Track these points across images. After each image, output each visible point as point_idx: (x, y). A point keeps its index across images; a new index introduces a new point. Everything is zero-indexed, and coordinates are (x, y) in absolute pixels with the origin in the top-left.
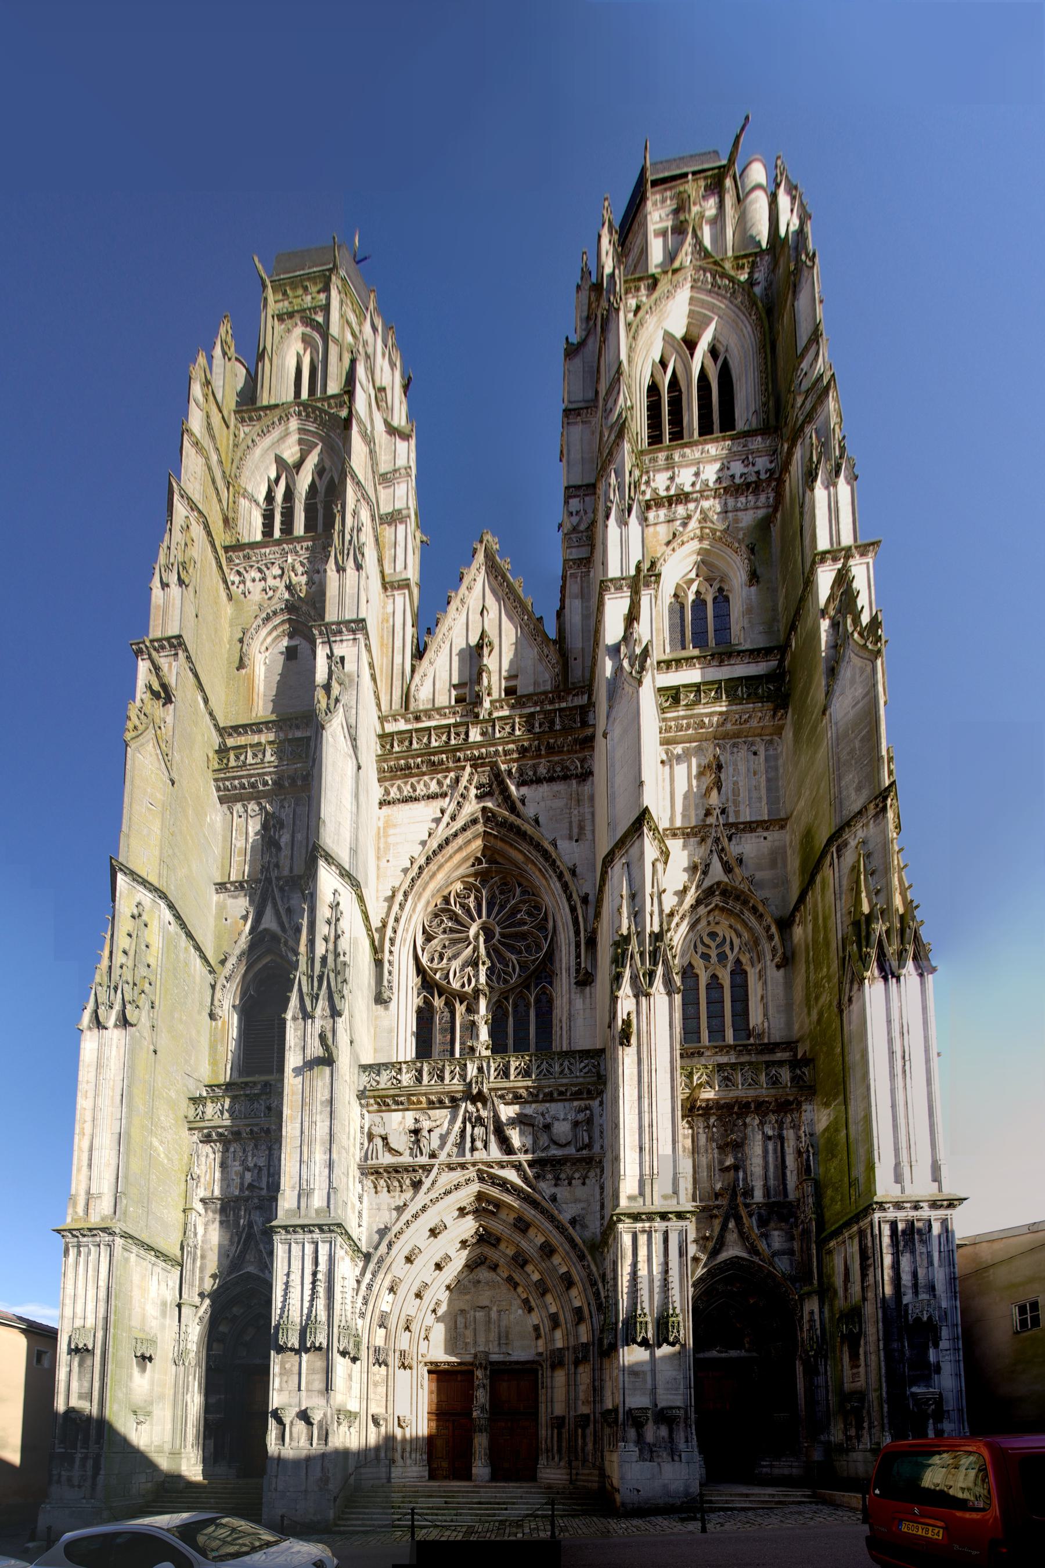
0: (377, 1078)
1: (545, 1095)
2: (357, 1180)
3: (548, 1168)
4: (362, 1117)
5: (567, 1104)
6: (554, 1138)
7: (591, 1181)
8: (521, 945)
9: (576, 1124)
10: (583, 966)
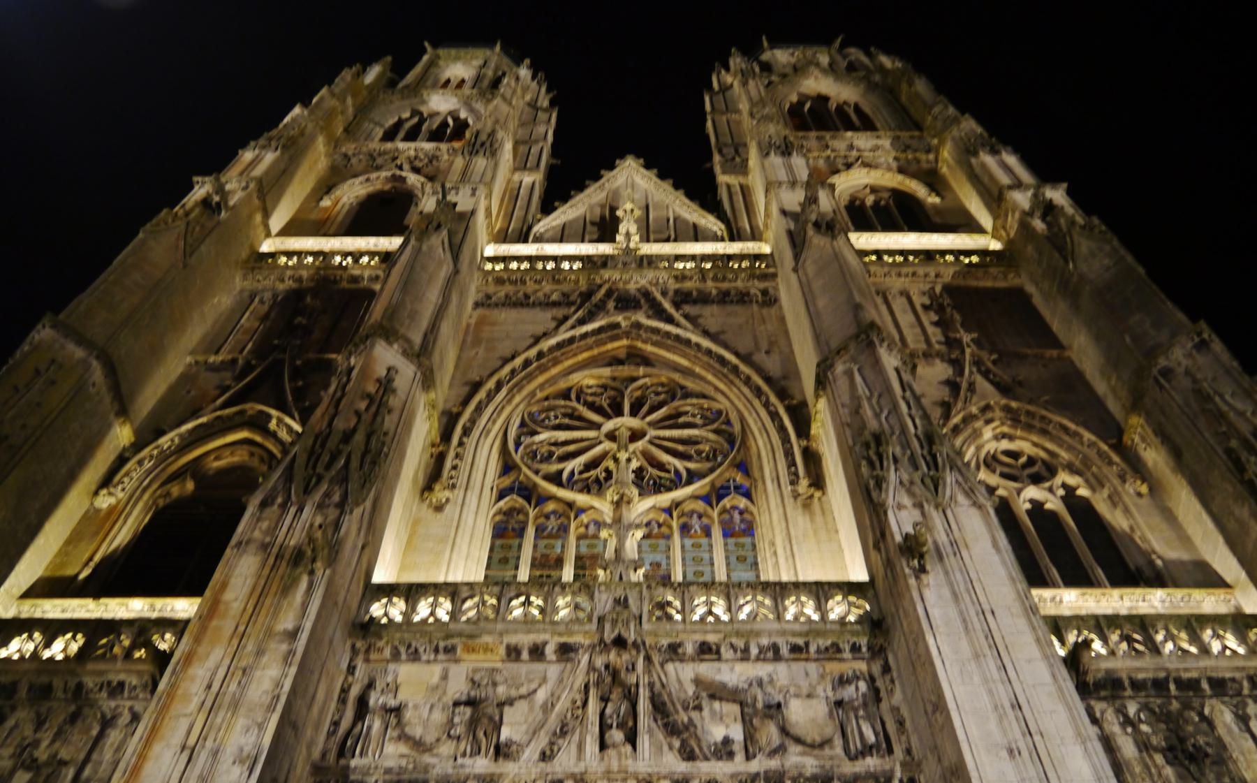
4: (351, 669)
5: (812, 667)
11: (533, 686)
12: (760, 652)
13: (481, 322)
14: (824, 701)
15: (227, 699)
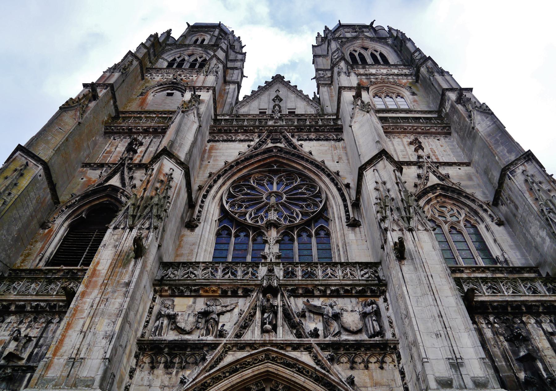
0: (176, 272)
1: (332, 291)
2: (133, 354)
3: (342, 352)
4: (154, 300)
5: (354, 300)
6: (346, 326)
7: (389, 366)
8: (304, 204)
9: (364, 315)
10: (351, 216)
11: (233, 306)
12: (331, 293)
13: (211, 148)
14: (358, 313)
15: (100, 311)
